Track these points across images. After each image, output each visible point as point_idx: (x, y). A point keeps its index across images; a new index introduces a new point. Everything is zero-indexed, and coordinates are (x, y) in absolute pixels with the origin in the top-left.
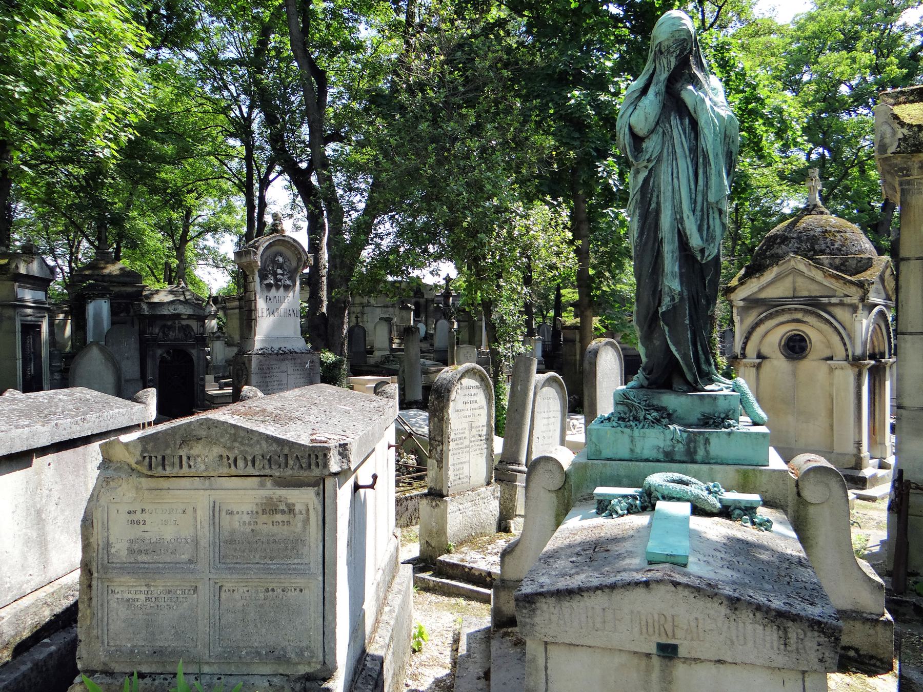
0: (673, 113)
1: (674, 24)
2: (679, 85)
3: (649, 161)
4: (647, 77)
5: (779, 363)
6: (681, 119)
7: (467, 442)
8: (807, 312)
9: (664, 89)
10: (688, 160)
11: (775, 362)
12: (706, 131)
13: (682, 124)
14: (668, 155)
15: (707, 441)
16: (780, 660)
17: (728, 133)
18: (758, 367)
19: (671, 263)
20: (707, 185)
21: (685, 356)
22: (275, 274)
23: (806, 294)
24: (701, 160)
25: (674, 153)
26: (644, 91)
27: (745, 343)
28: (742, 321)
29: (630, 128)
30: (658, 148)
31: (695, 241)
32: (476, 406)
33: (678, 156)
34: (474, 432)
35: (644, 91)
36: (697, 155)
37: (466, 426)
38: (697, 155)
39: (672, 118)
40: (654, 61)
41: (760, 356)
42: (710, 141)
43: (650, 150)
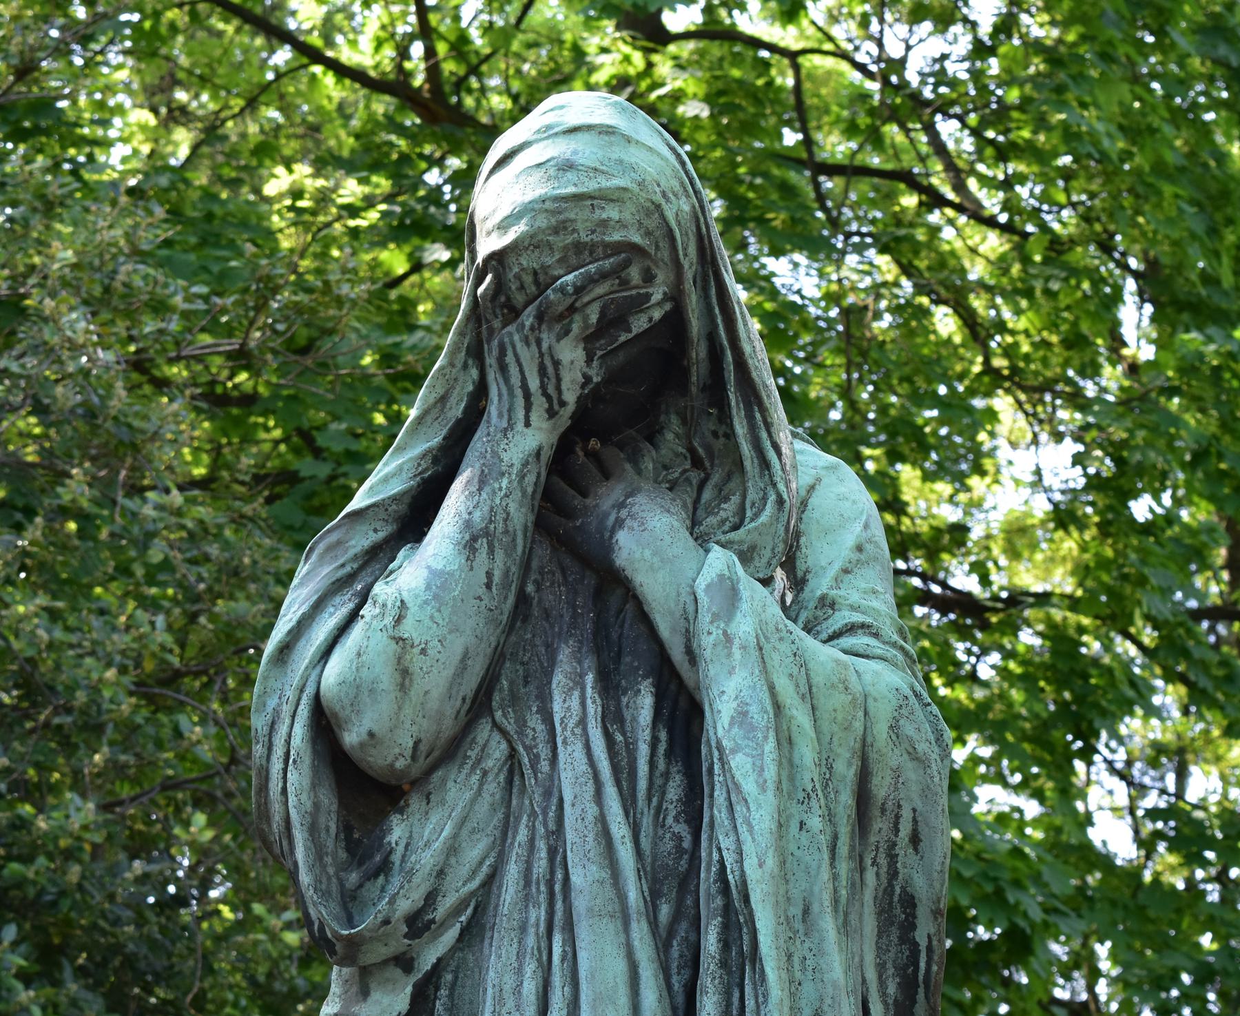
0: (565, 654)
1: (567, 166)
2: (607, 497)
3: (419, 924)
4: (433, 439)
6: (610, 686)
9: (520, 516)
10: (640, 932)
12: (740, 764)
13: (613, 718)
14: (527, 899)
17: (881, 787)
24: (711, 942)
25: (558, 887)
26: (414, 516)
29: (324, 723)
30: (475, 851)
33: (580, 904)
39: (559, 679)
40: (476, 352)
42: (758, 827)
43: (426, 860)
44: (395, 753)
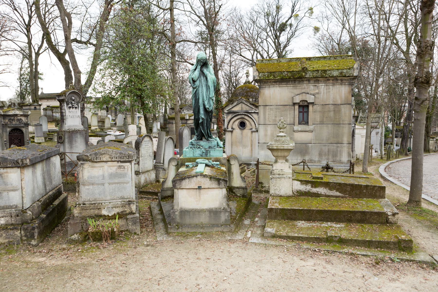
2: (203, 69)
5: (237, 131)
7: (146, 157)
8: (245, 115)
11: (236, 130)
15: (210, 152)
16: (218, 187)
18: (232, 132)
19: (202, 111)
20: (209, 93)
21: (205, 133)
22: (72, 103)
23: (245, 109)
26: (195, 69)
27: (228, 124)
28: (227, 117)
29: (192, 79)
31: (207, 106)
32: (148, 146)
34: (148, 154)
35: (195, 69)
36: (208, 87)
37: (146, 152)
38: (208, 87)
41: (232, 128)
44: (196, 80)
